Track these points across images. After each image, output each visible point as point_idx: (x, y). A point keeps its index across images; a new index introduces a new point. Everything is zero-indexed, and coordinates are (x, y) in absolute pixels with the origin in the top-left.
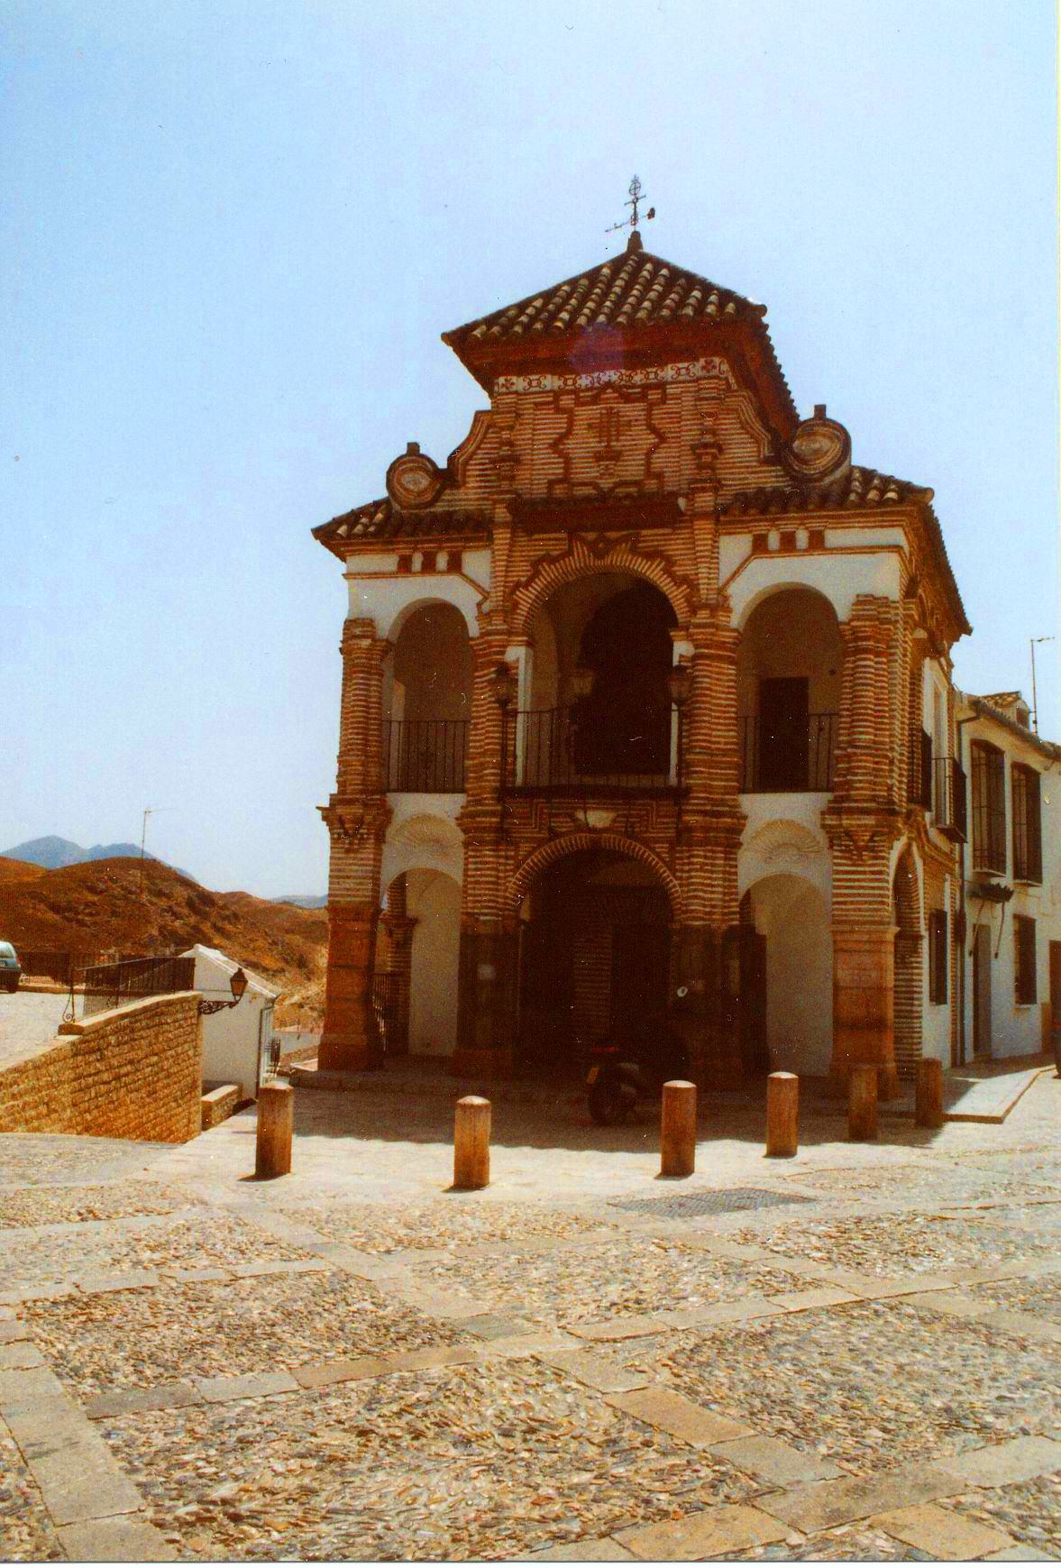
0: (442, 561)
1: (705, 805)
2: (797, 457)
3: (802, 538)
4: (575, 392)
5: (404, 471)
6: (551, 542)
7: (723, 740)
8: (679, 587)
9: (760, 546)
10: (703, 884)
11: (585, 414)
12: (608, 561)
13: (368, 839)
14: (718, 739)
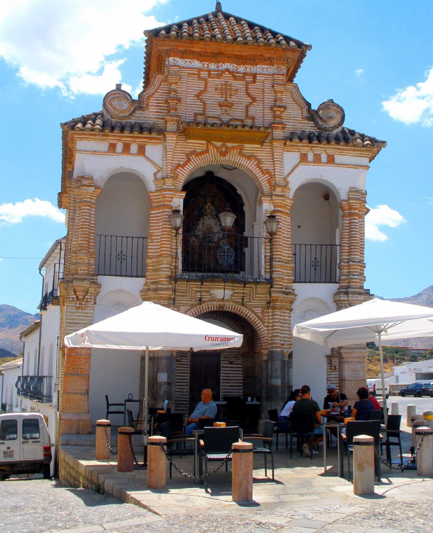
0: (134, 148)
1: (281, 288)
2: (321, 118)
3: (324, 158)
4: (209, 71)
5: (114, 98)
6: (198, 145)
7: (287, 255)
8: (264, 175)
9: (304, 158)
11: (214, 82)
12: (227, 158)
13: (90, 302)
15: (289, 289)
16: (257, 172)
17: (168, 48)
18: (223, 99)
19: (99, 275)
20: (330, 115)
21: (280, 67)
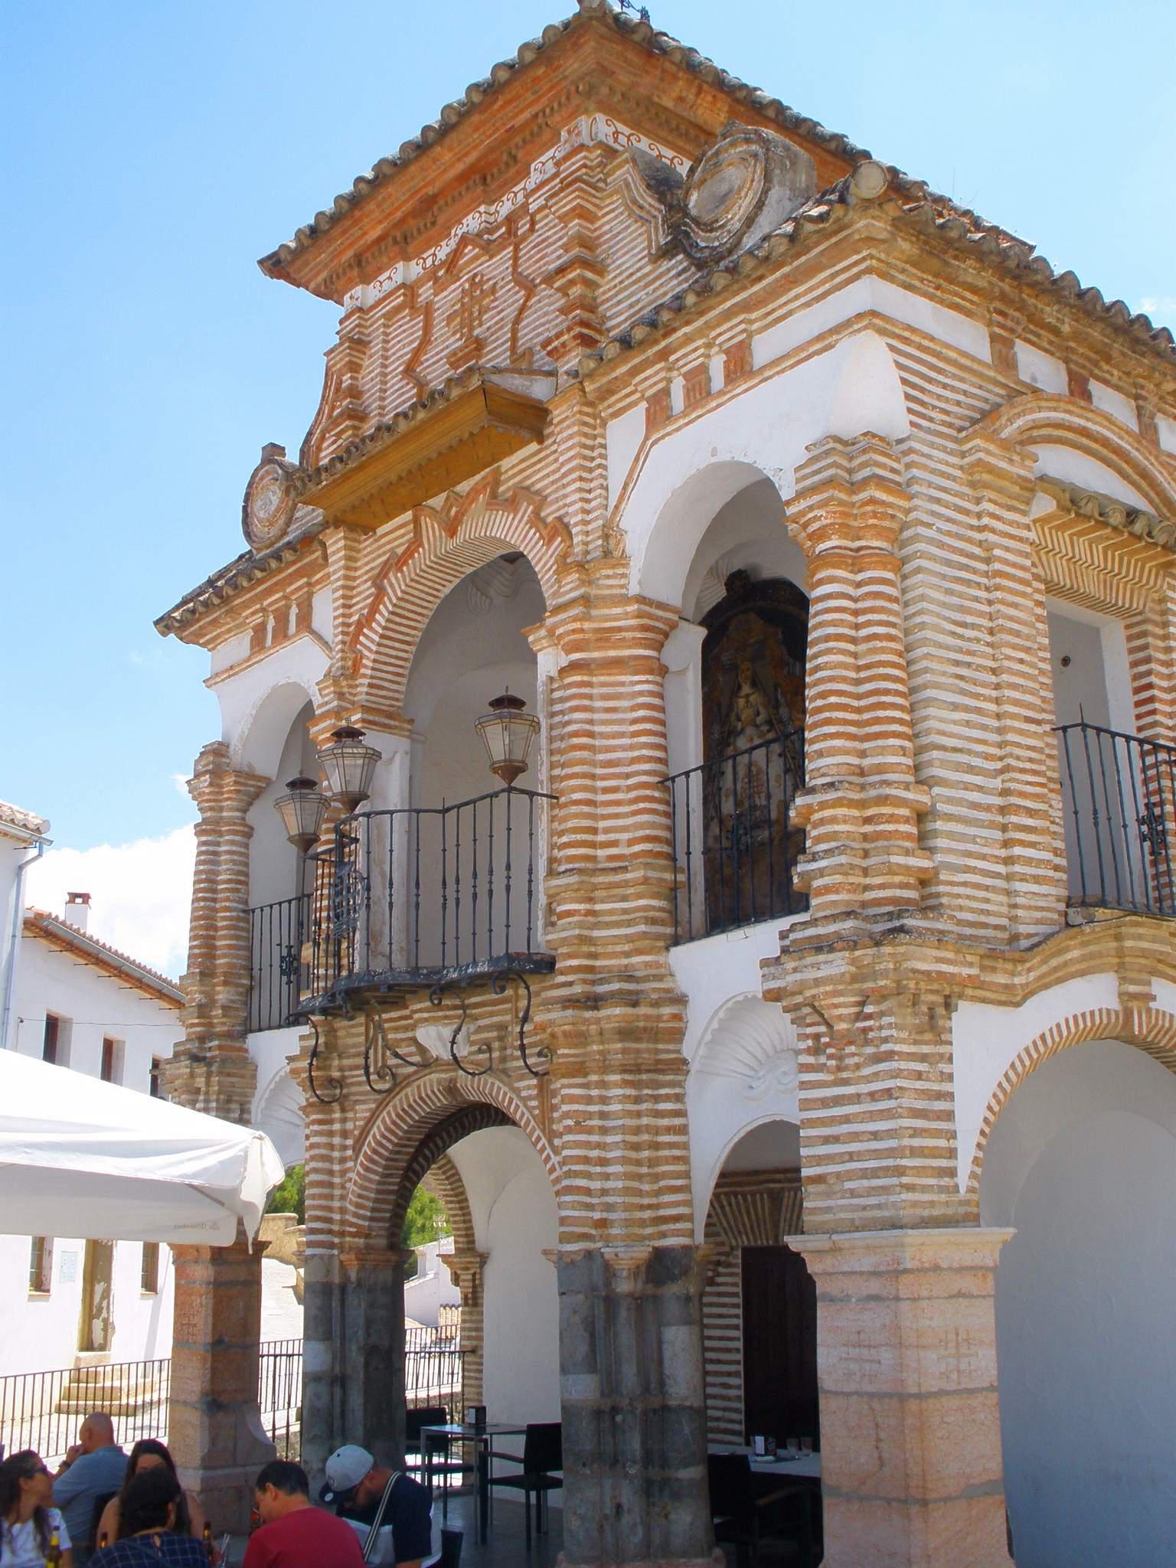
9: (659, 415)
10: (586, 1160)
12: (460, 538)
14: (612, 837)
17: (324, 275)
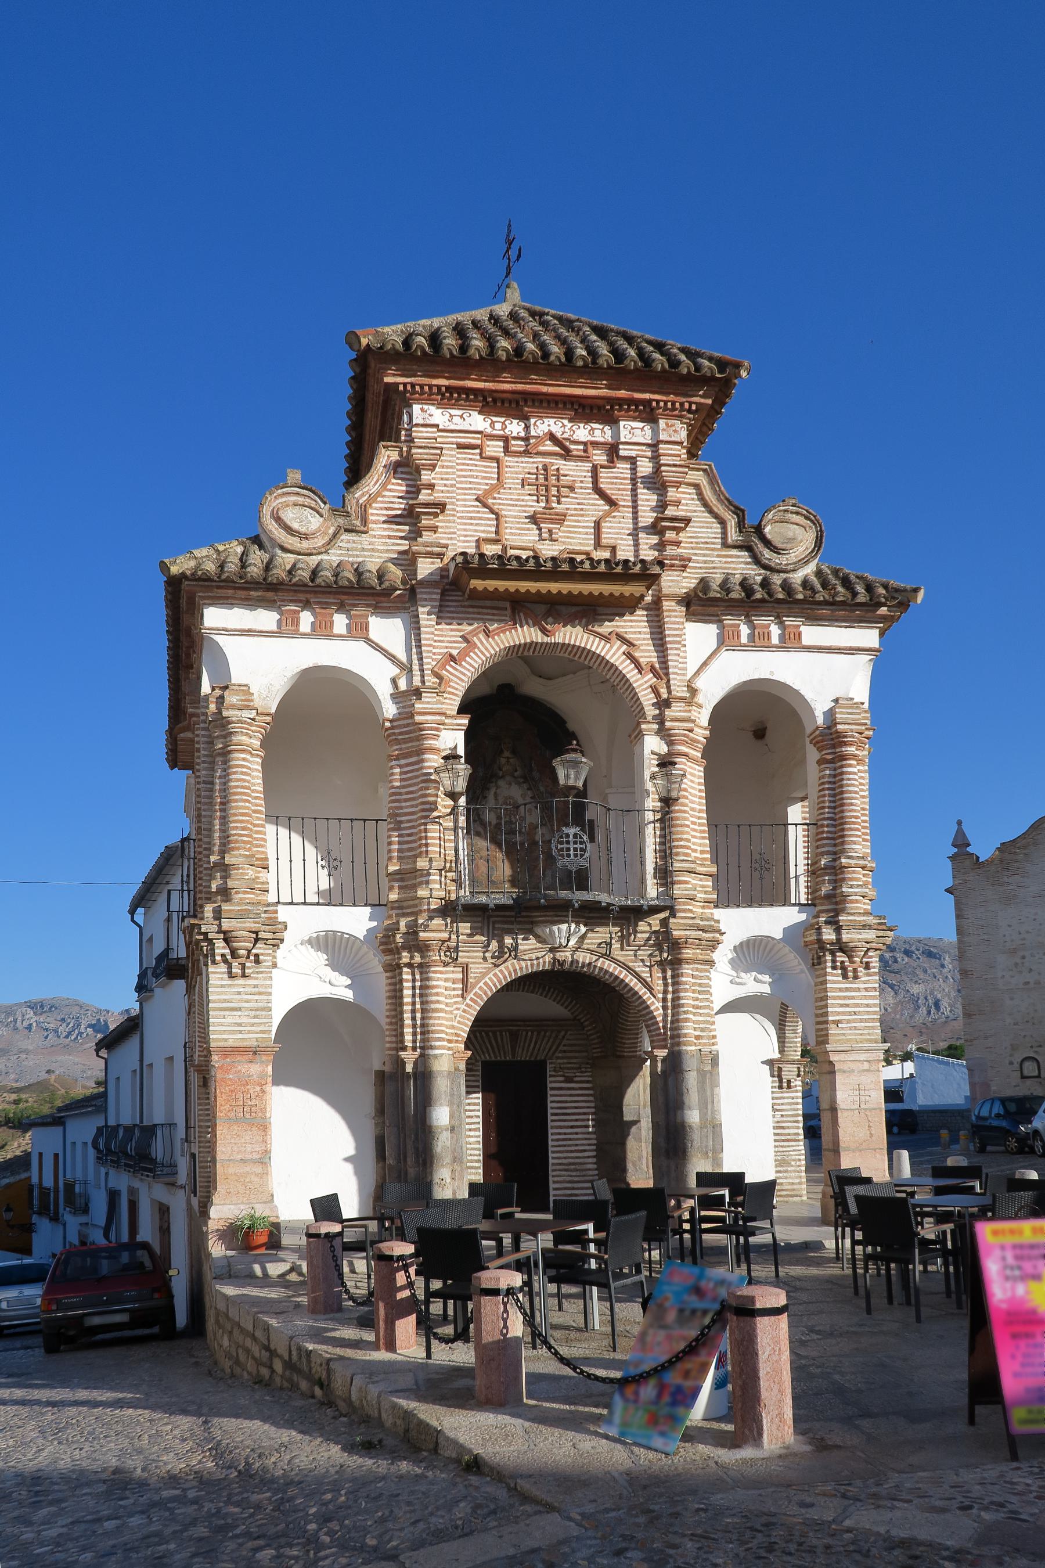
4: (506, 440)
11: (518, 467)
15: (708, 919)
16: (627, 668)
18: (543, 504)
19: (278, 902)
20: (790, 534)
21: (672, 426)
